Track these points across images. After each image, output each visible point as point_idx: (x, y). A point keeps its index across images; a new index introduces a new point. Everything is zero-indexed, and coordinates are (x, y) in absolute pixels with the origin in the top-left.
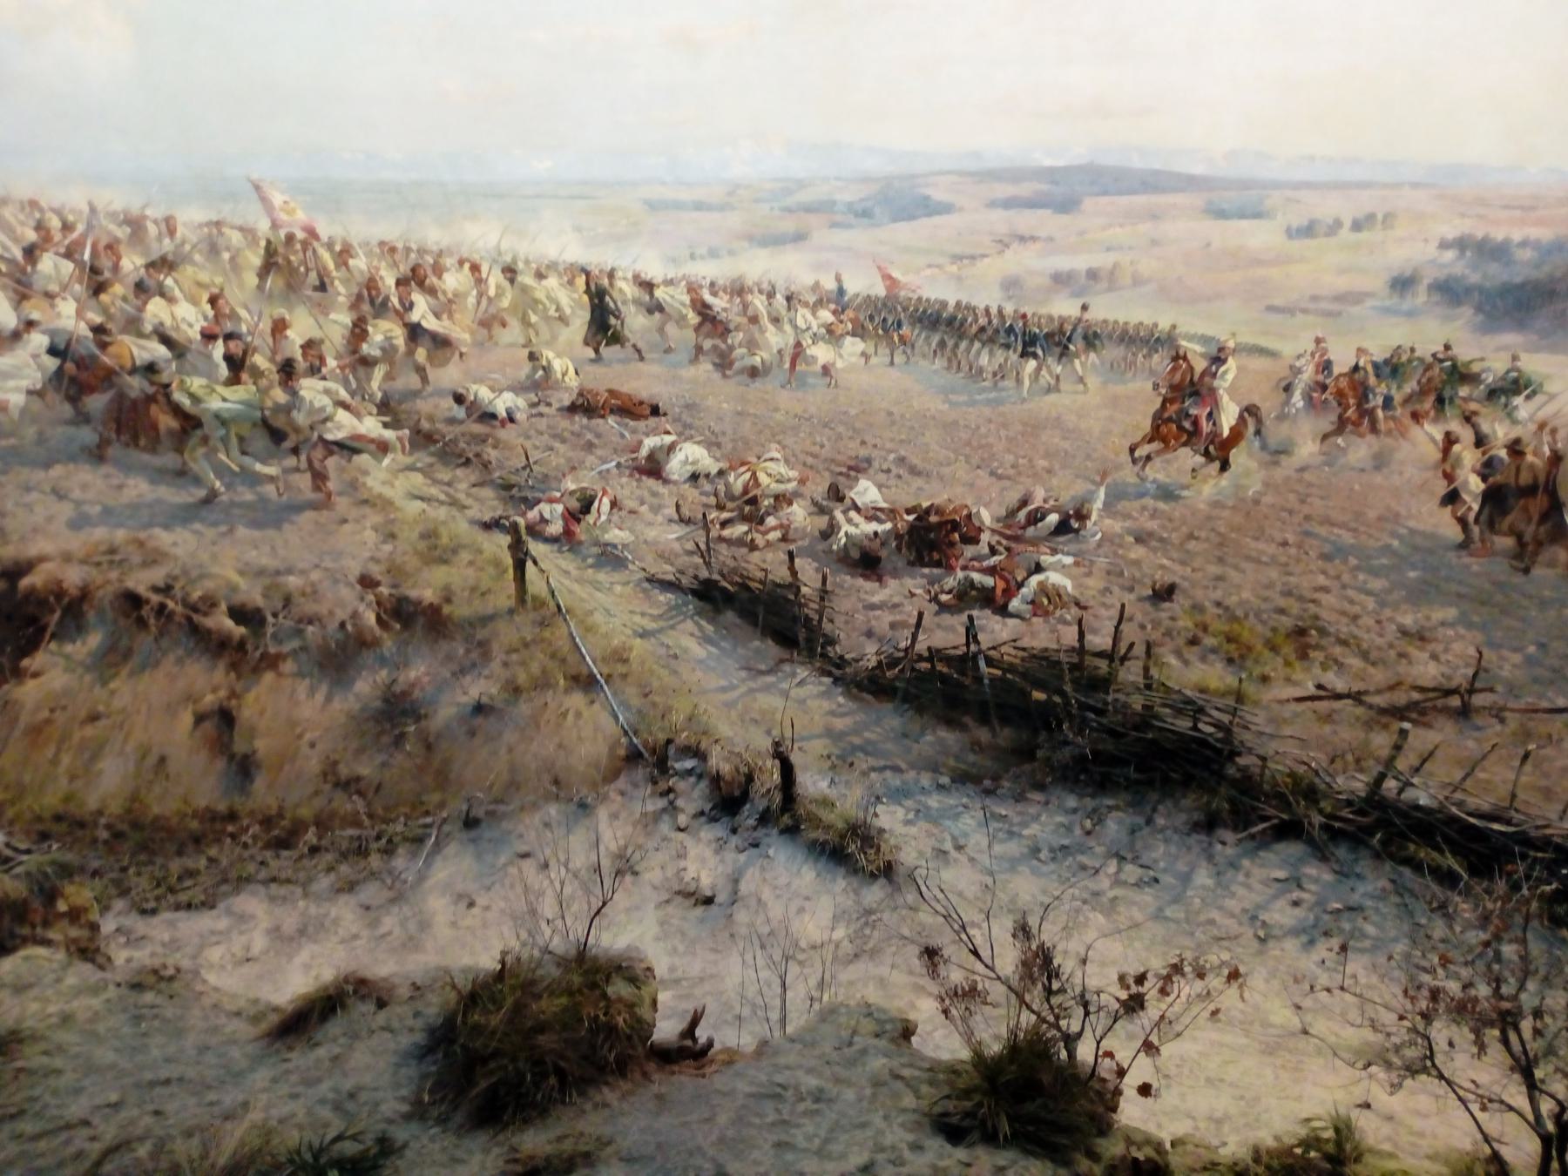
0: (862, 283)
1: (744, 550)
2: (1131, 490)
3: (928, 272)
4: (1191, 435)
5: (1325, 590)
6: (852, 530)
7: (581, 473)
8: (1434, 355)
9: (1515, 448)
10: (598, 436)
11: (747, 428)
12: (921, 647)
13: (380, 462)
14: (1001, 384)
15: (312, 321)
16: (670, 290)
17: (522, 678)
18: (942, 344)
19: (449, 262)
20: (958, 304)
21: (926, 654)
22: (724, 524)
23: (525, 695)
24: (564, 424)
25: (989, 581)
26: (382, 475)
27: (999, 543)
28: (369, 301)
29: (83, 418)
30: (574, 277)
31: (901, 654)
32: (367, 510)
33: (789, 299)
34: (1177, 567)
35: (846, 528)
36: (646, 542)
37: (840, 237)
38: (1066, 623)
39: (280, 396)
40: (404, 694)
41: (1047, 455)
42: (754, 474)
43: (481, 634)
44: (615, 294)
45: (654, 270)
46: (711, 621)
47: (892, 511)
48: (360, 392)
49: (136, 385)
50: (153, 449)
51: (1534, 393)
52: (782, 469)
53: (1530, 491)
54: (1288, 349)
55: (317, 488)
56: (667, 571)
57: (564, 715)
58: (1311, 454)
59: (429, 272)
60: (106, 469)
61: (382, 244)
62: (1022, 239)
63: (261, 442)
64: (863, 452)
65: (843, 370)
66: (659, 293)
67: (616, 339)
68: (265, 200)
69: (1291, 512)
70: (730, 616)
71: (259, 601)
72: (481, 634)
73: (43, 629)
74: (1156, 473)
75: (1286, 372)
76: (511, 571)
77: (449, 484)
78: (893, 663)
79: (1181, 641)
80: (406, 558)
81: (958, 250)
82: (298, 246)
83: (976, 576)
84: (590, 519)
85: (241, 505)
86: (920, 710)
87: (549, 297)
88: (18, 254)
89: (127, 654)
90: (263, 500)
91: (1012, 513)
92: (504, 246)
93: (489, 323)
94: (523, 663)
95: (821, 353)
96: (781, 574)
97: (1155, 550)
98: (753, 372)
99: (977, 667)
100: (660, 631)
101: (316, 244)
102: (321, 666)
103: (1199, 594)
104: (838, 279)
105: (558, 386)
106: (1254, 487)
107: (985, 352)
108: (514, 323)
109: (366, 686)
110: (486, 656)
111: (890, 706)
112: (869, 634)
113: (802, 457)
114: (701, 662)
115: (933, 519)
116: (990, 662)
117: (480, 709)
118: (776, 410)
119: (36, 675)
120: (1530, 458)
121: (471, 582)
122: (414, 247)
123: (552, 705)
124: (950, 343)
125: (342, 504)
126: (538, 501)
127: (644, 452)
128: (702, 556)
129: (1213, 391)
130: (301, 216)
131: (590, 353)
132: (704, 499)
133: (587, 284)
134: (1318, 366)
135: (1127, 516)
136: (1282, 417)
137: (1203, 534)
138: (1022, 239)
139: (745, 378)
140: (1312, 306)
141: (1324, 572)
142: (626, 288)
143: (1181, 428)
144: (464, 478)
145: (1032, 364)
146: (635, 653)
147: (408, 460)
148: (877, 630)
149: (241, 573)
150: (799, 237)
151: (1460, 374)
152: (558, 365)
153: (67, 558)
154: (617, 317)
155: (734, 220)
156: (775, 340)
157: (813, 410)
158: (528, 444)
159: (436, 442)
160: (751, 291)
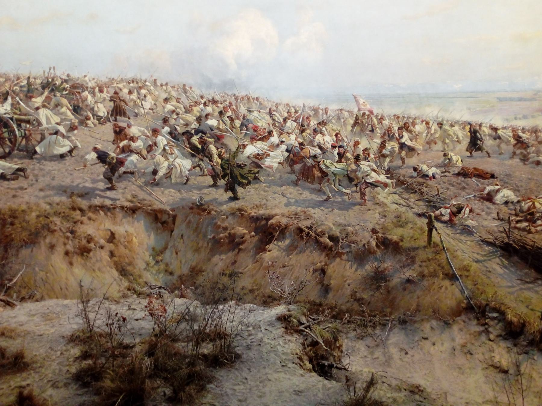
1: (525, 233)
7: (458, 198)
10: (468, 185)
11: (532, 185)
13: (384, 190)
15: (367, 142)
16: (504, 131)
17: (426, 272)
19: (418, 121)
22: (517, 222)
23: (426, 278)
24: (454, 180)
26: (385, 195)
28: (388, 135)
29: (293, 172)
30: (465, 126)
32: (377, 206)
36: (482, 226)
39: (354, 167)
40: (383, 272)
42: (534, 204)
43: (412, 254)
44: (481, 132)
45: (498, 123)
46: (506, 259)
48: (380, 166)
49: (310, 162)
50: (312, 183)
55: (362, 198)
56: (490, 238)
57: (441, 288)
59: (410, 125)
60: (297, 188)
61: (395, 115)
63: (345, 182)
66: (499, 132)
67: (480, 149)
68: (357, 102)
70: (516, 258)
71: (338, 235)
72: (412, 254)
73: (274, 236)
76: (427, 232)
77: (407, 199)
80: (389, 224)
82: (366, 117)
84: (460, 216)
85: (336, 202)
87: (454, 134)
88: (281, 120)
89: (296, 248)
90: (344, 201)
92: (439, 115)
93: (430, 143)
94: (427, 266)
100: (484, 261)
101: (372, 116)
102: (355, 258)
105: (454, 166)
108: (440, 144)
109: (369, 267)
110: (413, 262)
114: (500, 275)
117: (409, 281)
119: (269, 251)
121: (411, 235)
122: (406, 116)
123: (436, 284)
125: (369, 204)
126: (440, 208)
127: (486, 192)
128: (506, 234)
130: (368, 107)
131: (468, 154)
132: (510, 211)
133: (470, 129)
139: (534, 165)
142: (486, 130)
144: (413, 197)
146: (472, 268)
147: (394, 190)
149: (334, 224)
152: (454, 158)
153: (283, 215)
154: (481, 141)
158: (439, 187)
159: (405, 184)
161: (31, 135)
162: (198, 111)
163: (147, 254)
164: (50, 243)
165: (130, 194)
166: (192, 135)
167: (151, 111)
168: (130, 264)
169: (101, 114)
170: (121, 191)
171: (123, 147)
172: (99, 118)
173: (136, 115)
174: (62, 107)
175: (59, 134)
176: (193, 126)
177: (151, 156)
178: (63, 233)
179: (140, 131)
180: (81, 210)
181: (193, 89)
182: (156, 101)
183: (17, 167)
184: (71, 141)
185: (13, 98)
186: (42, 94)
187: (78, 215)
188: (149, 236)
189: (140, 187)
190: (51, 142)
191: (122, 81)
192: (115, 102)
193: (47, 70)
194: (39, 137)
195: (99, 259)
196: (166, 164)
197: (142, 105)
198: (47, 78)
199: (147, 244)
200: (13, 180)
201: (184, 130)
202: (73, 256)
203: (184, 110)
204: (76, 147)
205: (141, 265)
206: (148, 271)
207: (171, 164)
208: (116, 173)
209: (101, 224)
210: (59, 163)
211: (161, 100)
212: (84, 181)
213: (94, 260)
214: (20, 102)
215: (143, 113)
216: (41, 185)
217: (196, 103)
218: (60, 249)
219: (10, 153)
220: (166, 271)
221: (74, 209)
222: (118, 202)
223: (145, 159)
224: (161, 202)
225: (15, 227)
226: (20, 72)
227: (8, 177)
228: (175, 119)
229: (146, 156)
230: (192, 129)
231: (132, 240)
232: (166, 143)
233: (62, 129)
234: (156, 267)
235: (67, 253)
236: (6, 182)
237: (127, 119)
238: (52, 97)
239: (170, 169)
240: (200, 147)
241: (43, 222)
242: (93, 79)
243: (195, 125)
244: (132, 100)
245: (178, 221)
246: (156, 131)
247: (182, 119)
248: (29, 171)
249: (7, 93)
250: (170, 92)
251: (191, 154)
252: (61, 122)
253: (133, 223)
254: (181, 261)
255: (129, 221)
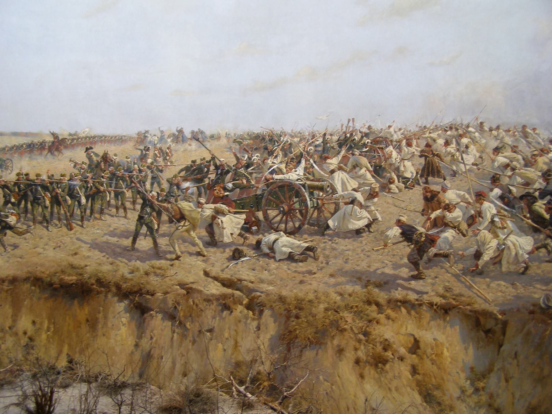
161: (323, 204)
162: (545, 163)
163: (463, 375)
164: (338, 346)
165: (442, 286)
166: (535, 200)
167: (475, 167)
168: (438, 387)
169: (408, 175)
170: (430, 281)
171: (435, 219)
172: (405, 180)
173: (454, 174)
174: (361, 169)
175: (356, 203)
176: (537, 186)
177: (473, 231)
178: (355, 334)
179: (459, 196)
180: (378, 304)
181: (537, 131)
182: (482, 152)
183: (306, 245)
184: (370, 212)
185: (306, 160)
186: (339, 153)
187: (373, 311)
188: (466, 349)
189: (456, 276)
190: (346, 214)
191: (436, 128)
192: (426, 157)
193: (345, 124)
194: (332, 207)
195: (397, 374)
196: (494, 243)
197: (462, 159)
198: (345, 133)
199: (463, 360)
200: (301, 261)
201: (523, 192)
202: (365, 367)
203: (522, 162)
204: (375, 220)
205: (453, 391)
206: (464, 401)
207: (501, 242)
208: (425, 255)
209: (402, 325)
210: (354, 241)
211: (489, 151)
212: (384, 265)
213: (390, 375)
214: (314, 165)
215: (464, 170)
216: (331, 269)
217: (542, 150)
218: (350, 355)
219: (300, 227)
220: (490, 405)
221: (369, 303)
222: (425, 296)
223: (464, 235)
224: (486, 300)
225: (300, 320)
226: (315, 129)
227: (296, 258)
228: (510, 177)
229: (467, 231)
230: (536, 190)
231: (442, 353)
232: (494, 211)
233: (359, 197)
234: (475, 398)
235: (357, 362)
236: (294, 264)
237: (442, 180)
238: (350, 156)
239: (501, 250)
240: (547, 216)
241: (331, 318)
242: (400, 129)
243: (540, 183)
244: (450, 153)
245: (510, 331)
246: (481, 195)
247: (520, 175)
248: (319, 250)
249: (301, 155)
250: (503, 138)
251: (533, 227)
252: (359, 188)
253: (445, 328)
254: (513, 394)
255: (439, 325)
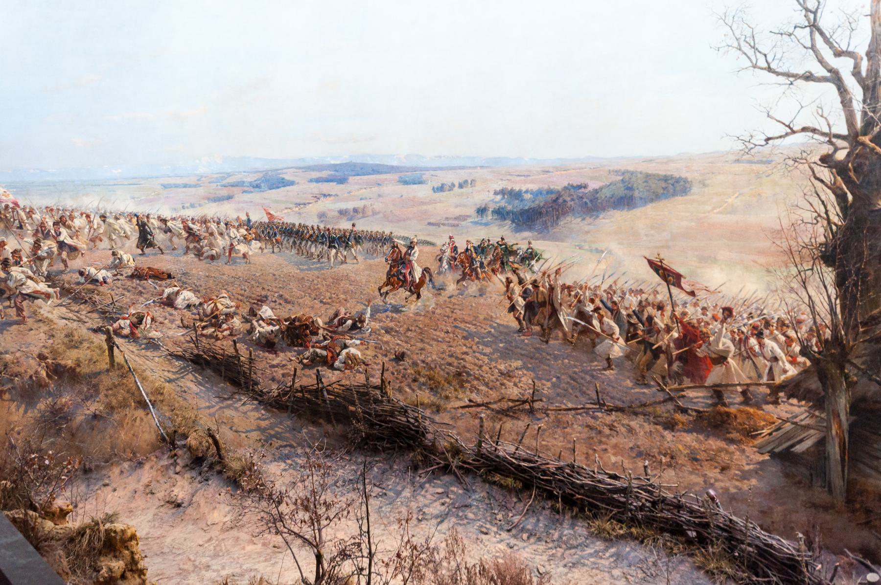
0: (259, 216)
1: (213, 340)
2: (381, 308)
3: (286, 211)
4: (403, 283)
5: (466, 353)
6: (261, 330)
8: (497, 243)
9: (535, 284)
10: (144, 288)
11: (211, 283)
12: (297, 385)
13: (47, 303)
14: (321, 260)
15: (16, 242)
16: (174, 222)
17: (114, 402)
18: (294, 243)
19: (76, 214)
20: (300, 224)
21: (300, 389)
22: (204, 328)
23: (116, 411)
24: (129, 283)
25: (324, 353)
26: (48, 309)
27: (327, 334)
28: (42, 232)
30: (131, 218)
31: (288, 389)
32: (41, 324)
33: (226, 224)
34: (404, 344)
35: (258, 329)
36: (168, 337)
37: (247, 197)
38: (360, 372)
40: (61, 409)
41: (345, 293)
42: (216, 304)
43: (94, 381)
44: (150, 225)
45: (167, 214)
46: (200, 374)
47: (279, 320)
48: (37, 272)
51: (539, 258)
52: (228, 301)
53: (543, 304)
54: (439, 242)
55: (18, 315)
56: (179, 351)
57: (135, 420)
58: (454, 290)
59: (68, 219)
61: (47, 208)
62: (325, 195)
64: (263, 293)
65: (252, 256)
66: (169, 224)
67: (151, 245)
69: (448, 317)
70: (209, 372)
72: (94, 381)
74: (391, 300)
75: (439, 252)
76: (107, 351)
77: (77, 312)
78: (285, 393)
79: (410, 380)
80: (59, 346)
81: (298, 201)
82: (10, 210)
83: (318, 350)
84: (142, 327)
86: (300, 416)
91: (331, 320)
92: (101, 206)
93: (94, 240)
94: (114, 395)
95: (242, 248)
96: (231, 351)
97: (393, 336)
98: (213, 258)
99: (323, 396)
100: (177, 379)
101: (18, 209)
102: (22, 397)
103: (415, 357)
104: (247, 215)
105: (126, 267)
106: (432, 306)
107: (313, 245)
108: (105, 239)
110: (97, 392)
111: (286, 415)
112: (273, 379)
113: (237, 296)
114: (197, 394)
115: (297, 323)
116: (329, 392)
117: (95, 416)
118: (224, 274)
120: (541, 289)
121: (89, 357)
122: (61, 208)
123: (129, 416)
124: (298, 242)
125: (30, 321)
126: (119, 319)
127: (165, 295)
128: (194, 344)
129: (410, 261)
130: (12, 197)
131: (139, 251)
133: (137, 221)
134: (452, 249)
135: (381, 321)
136: (439, 273)
137: (413, 328)
138: (325, 195)
140: (447, 222)
141: (465, 345)
142: (155, 223)
143: (399, 279)
144: (84, 309)
145: (334, 251)
146: (166, 390)
147: (59, 302)
148: (277, 377)
150: (229, 198)
151: (509, 251)
152: (125, 257)
154: (151, 235)
155: (201, 191)
156: (221, 243)
157: (240, 274)
158: (113, 293)
159: (72, 293)
160: (209, 222)
